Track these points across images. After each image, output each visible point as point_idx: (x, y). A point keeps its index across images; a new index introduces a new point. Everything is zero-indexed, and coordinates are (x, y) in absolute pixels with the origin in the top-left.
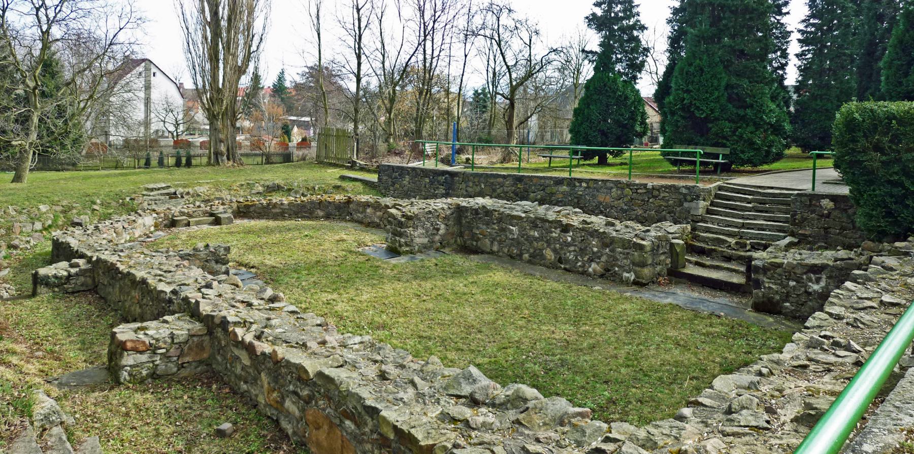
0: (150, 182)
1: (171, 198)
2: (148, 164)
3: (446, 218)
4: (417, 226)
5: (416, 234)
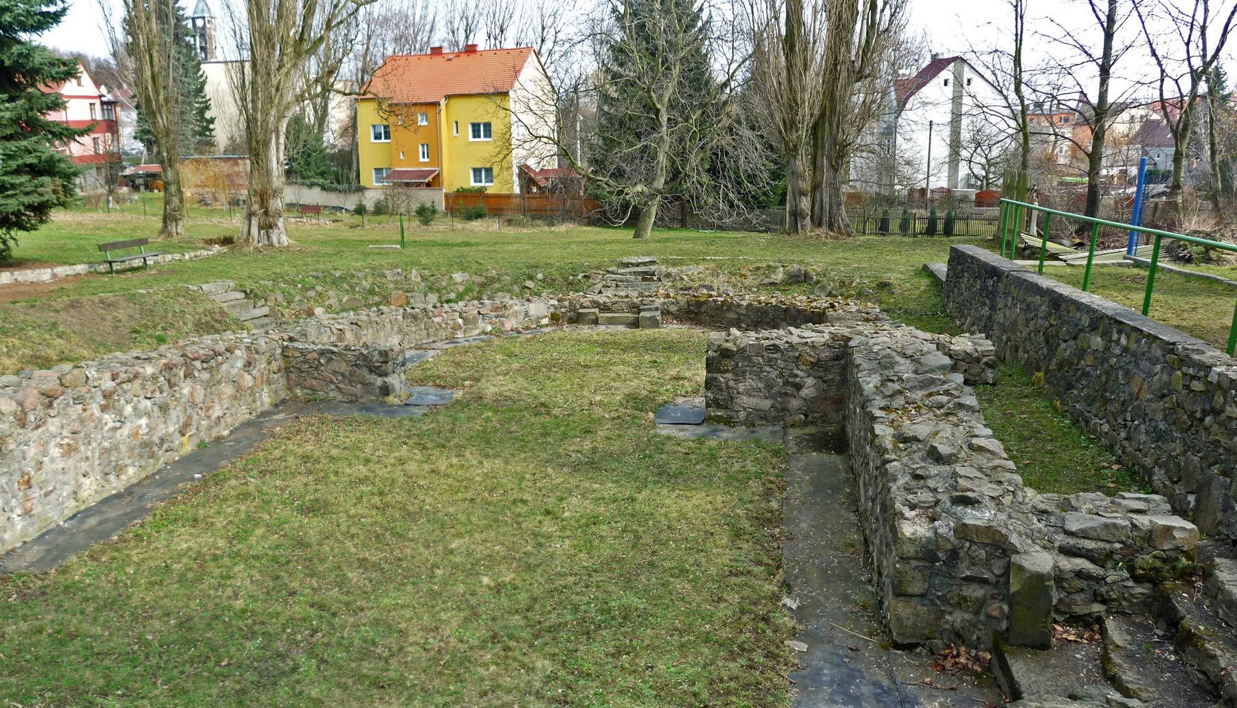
0: (629, 254)
1: (644, 279)
2: (883, 228)
3: (816, 365)
4: (744, 372)
5: (741, 387)
